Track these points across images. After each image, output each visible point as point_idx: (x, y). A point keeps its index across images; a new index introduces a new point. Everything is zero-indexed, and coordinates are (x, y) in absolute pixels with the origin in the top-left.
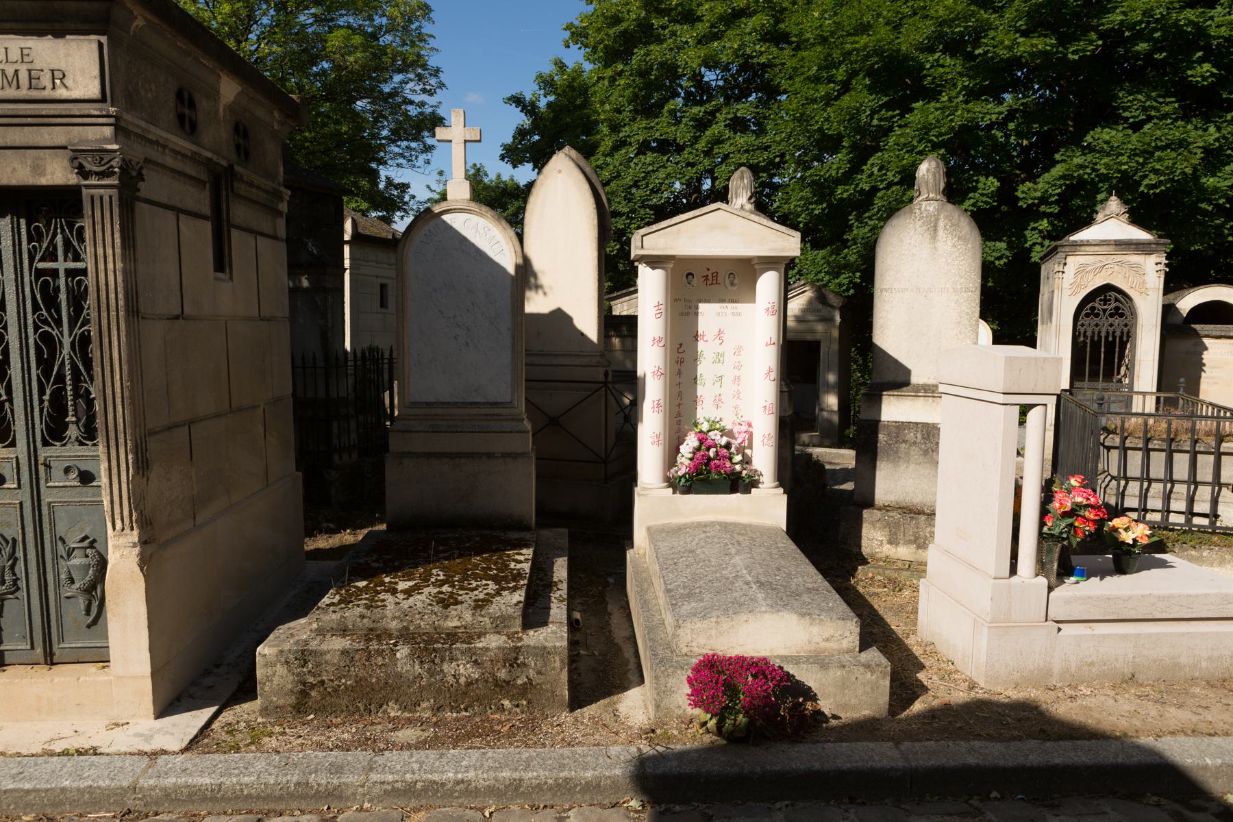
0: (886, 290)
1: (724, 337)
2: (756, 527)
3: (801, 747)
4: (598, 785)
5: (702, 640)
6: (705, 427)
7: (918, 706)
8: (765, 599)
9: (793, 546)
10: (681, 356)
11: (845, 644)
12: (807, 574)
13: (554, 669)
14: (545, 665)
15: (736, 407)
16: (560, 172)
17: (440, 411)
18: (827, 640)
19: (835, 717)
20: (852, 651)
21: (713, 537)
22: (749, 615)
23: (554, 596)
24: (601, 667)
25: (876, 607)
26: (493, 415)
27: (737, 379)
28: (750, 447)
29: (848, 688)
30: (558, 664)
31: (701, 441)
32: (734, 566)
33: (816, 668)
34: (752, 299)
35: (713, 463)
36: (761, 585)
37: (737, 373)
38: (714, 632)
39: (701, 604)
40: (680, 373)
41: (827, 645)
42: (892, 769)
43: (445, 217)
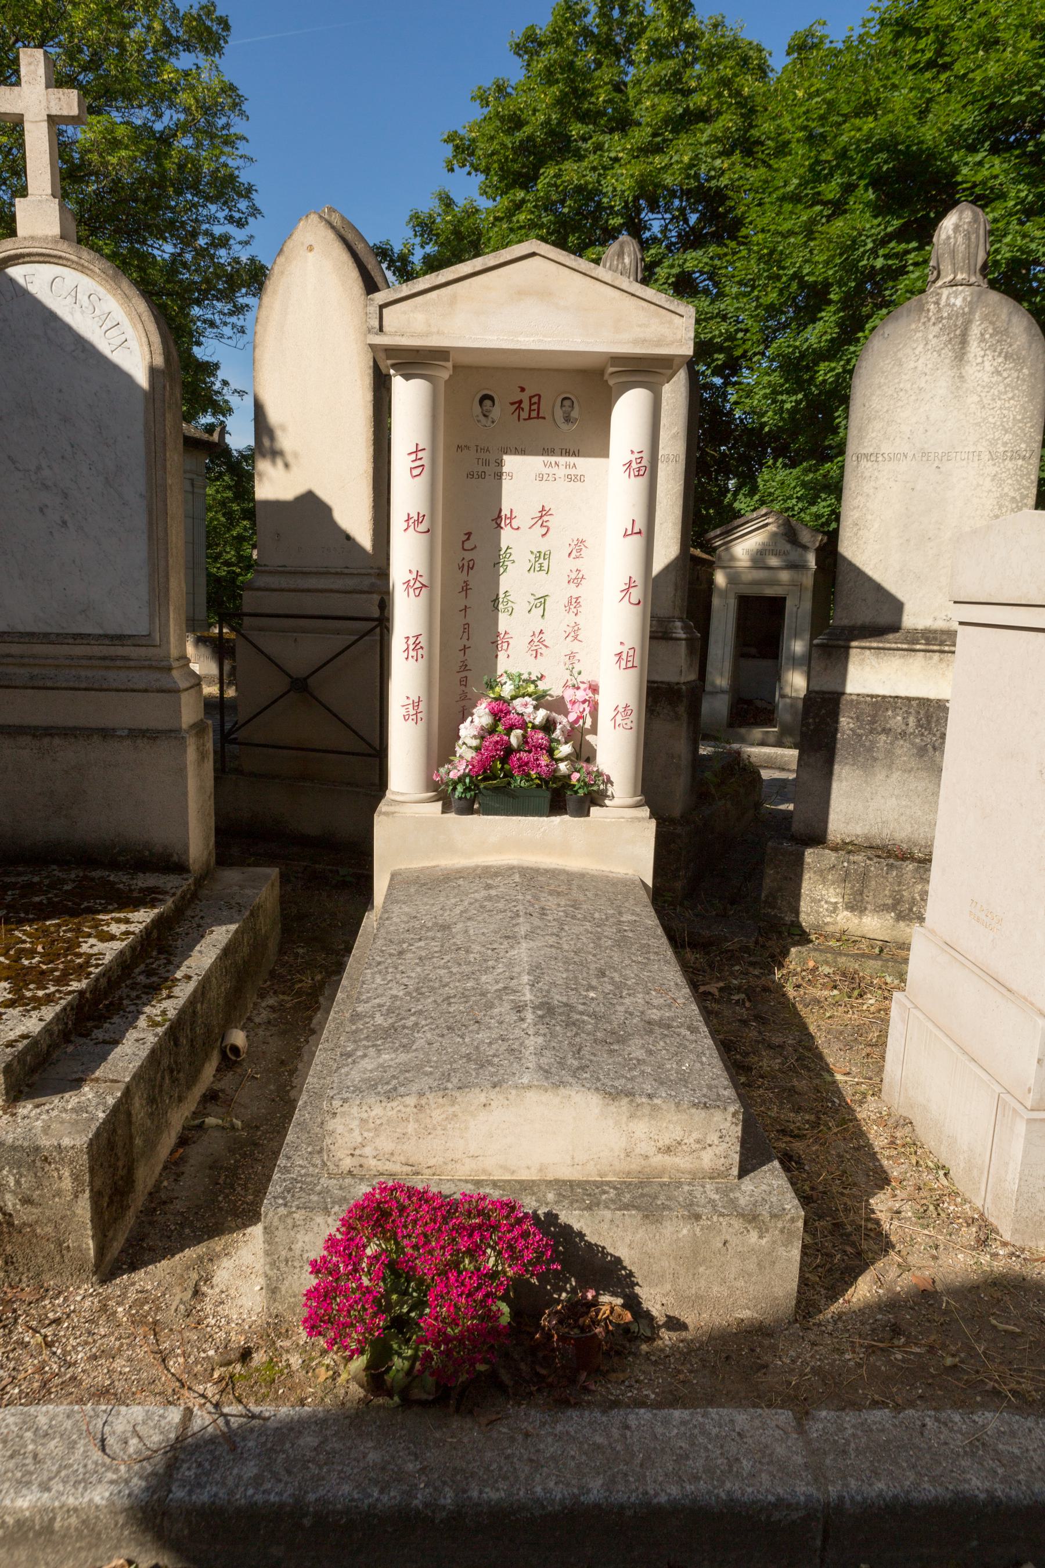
0: (867, 457)
1: (552, 522)
2: (593, 878)
3: (574, 1422)
4: (48, 1529)
5: (385, 1143)
6: (507, 690)
7: (863, 1290)
8: (539, 1053)
9: (651, 920)
10: (468, 556)
11: (707, 1159)
12: (659, 984)
13: (58, 1193)
14: (40, 1186)
15: (571, 656)
16: (310, 248)
17: (15, 649)
18: (668, 1150)
19: (674, 1324)
20: (714, 1175)
21: (498, 898)
22: (493, 1094)
23: (153, 1010)
24: (167, 1194)
25: (812, 1029)
26: (113, 659)
27: (574, 604)
28: (594, 730)
29: (712, 1259)
30: (67, 1184)
31: (498, 715)
32: (510, 965)
33: (632, 1217)
34: (603, 451)
35: (515, 758)
36: (547, 1010)
37: (573, 591)
38: (411, 1127)
39: (403, 1057)
40: (466, 588)
41: (668, 1160)
42: (780, 1503)
43: (16, 272)
